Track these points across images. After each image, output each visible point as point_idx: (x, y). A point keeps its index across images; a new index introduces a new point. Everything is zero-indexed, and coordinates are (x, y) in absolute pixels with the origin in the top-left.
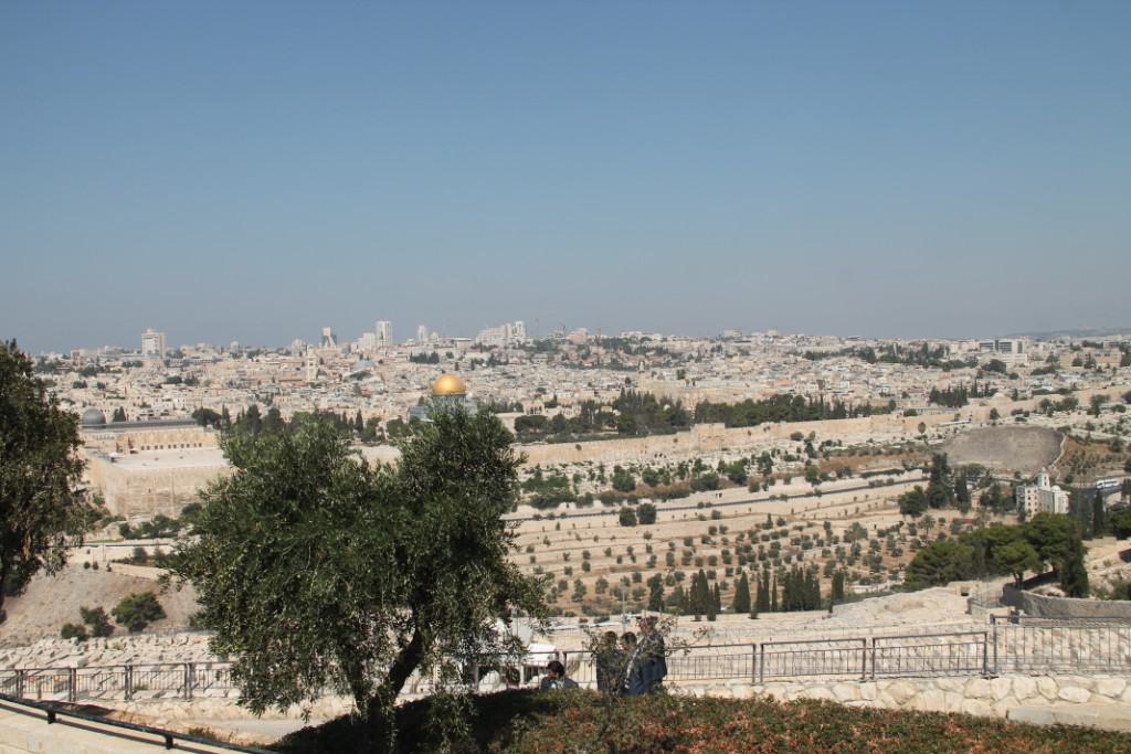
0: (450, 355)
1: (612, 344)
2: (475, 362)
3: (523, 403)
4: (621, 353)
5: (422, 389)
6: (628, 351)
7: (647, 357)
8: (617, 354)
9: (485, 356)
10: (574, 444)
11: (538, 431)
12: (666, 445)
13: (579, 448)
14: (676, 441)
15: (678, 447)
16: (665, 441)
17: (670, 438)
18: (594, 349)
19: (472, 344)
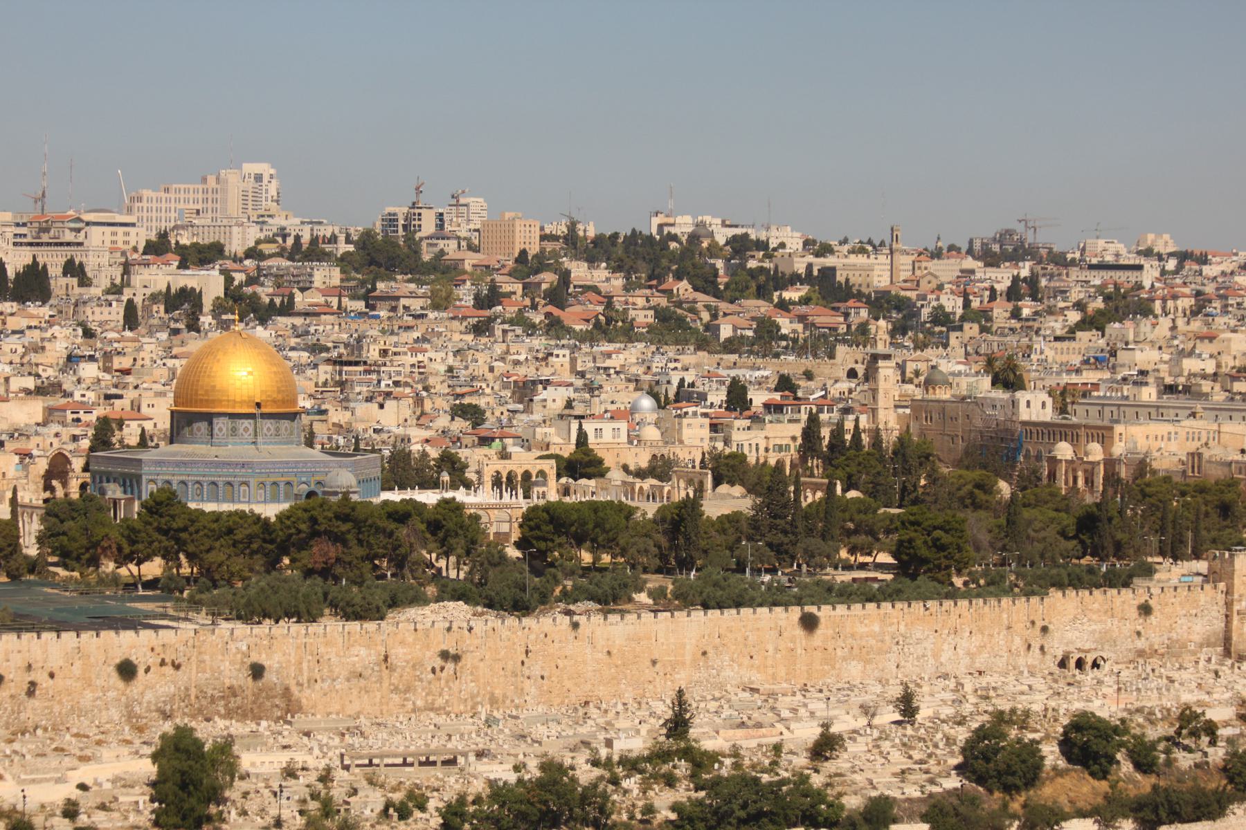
0: (73, 269)
1: (642, 256)
2: (183, 302)
3: (463, 454)
4: (683, 288)
5: (40, 391)
6: (706, 283)
7: (783, 306)
8: (668, 293)
9: (209, 283)
10: (796, 612)
11: (606, 558)
12: (1112, 624)
13: (809, 623)
14: (1145, 610)
15: (1155, 632)
16: (1111, 613)
17: (1125, 600)
18: (579, 271)
19: (140, 236)
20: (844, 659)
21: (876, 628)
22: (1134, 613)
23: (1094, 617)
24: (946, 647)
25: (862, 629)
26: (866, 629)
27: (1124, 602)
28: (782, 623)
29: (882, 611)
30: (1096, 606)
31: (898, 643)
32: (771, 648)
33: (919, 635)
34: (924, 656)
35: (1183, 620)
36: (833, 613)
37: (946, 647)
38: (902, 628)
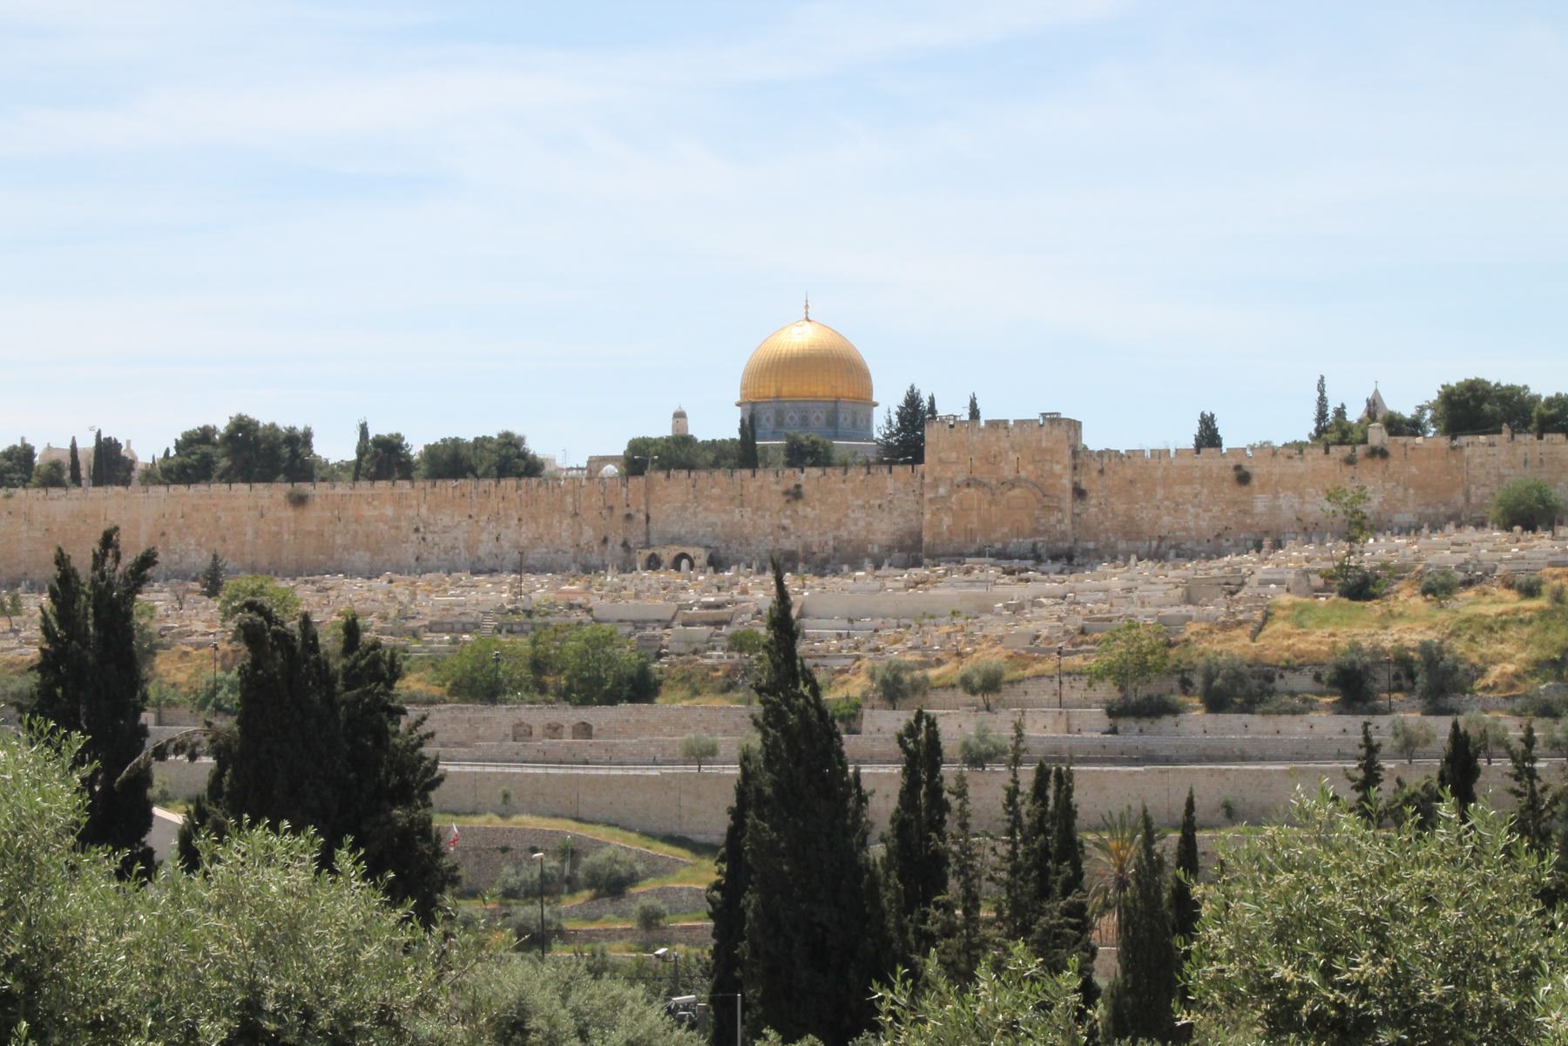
20: (346, 548)
21: (389, 511)
22: (777, 502)
23: (713, 506)
24: (484, 536)
25: (369, 512)
26: (376, 513)
27: (761, 487)
28: (265, 502)
29: (397, 491)
30: (716, 491)
31: (417, 530)
32: (250, 531)
33: (447, 520)
34: (453, 548)
35: (859, 514)
36: (330, 492)
37: (484, 536)
38: (424, 510)
